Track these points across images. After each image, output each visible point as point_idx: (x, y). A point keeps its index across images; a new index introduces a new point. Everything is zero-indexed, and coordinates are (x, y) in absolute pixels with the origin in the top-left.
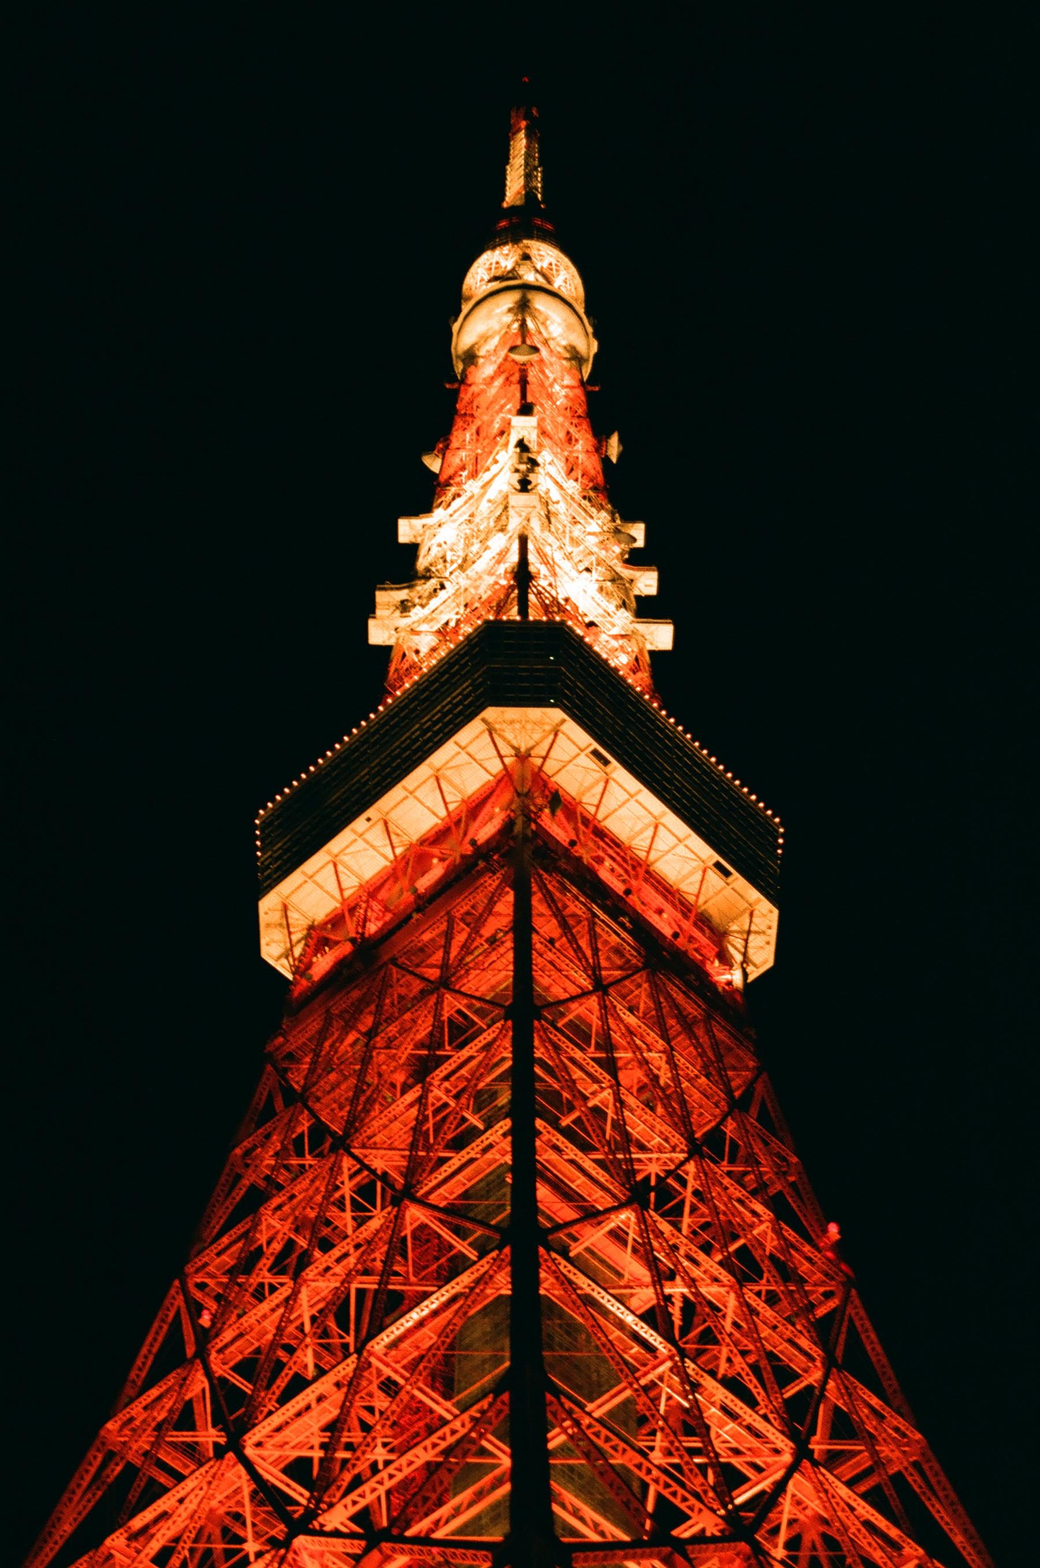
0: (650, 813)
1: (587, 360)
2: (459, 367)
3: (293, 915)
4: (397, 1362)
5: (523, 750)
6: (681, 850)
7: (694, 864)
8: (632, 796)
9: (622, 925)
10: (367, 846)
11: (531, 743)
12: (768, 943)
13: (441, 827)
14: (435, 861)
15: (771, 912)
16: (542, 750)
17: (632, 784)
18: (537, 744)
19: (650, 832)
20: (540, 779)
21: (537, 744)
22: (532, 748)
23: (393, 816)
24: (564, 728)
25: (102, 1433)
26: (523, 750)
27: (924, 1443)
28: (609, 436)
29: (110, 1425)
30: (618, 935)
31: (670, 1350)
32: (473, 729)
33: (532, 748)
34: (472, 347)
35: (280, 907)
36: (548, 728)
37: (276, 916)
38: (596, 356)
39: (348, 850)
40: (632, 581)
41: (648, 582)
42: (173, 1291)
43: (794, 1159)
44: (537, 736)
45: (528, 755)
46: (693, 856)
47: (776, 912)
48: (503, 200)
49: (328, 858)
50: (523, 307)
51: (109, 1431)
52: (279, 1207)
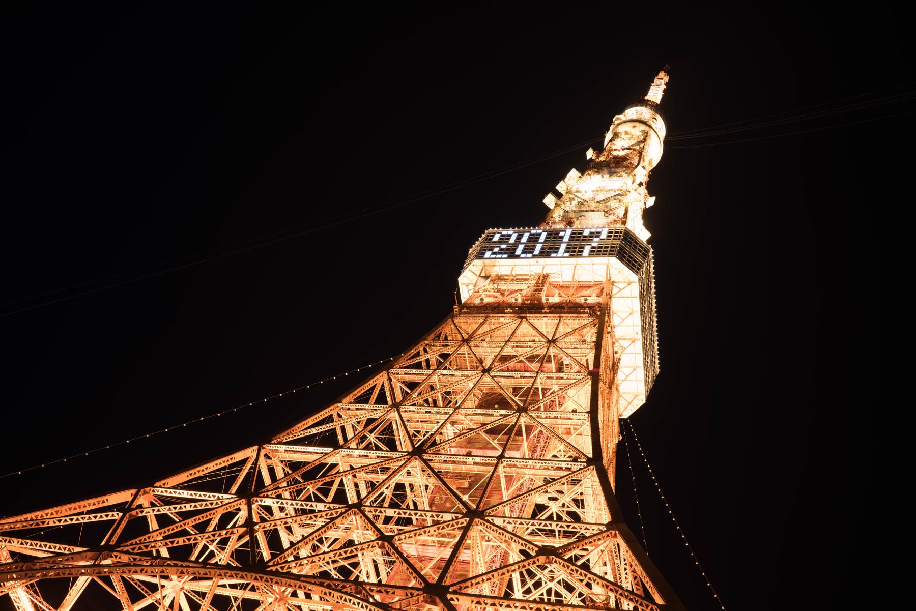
4: (504, 472)
5: (612, 280)
11: (617, 281)
12: (632, 410)
13: (561, 284)
14: (557, 295)
15: (642, 401)
16: (621, 286)
18: (619, 282)
20: (610, 296)
21: (619, 282)
22: (616, 282)
24: (633, 284)
25: (336, 405)
26: (612, 280)
29: (340, 405)
33: (616, 282)
34: (619, 133)
36: (627, 281)
39: (520, 267)
42: (381, 374)
44: (620, 280)
45: (613, 283)
46: (634, 363)
47: (644, 402)
48: (646, 95)
49: (513, 264)
51: (338, 407)
52: (443, 375)
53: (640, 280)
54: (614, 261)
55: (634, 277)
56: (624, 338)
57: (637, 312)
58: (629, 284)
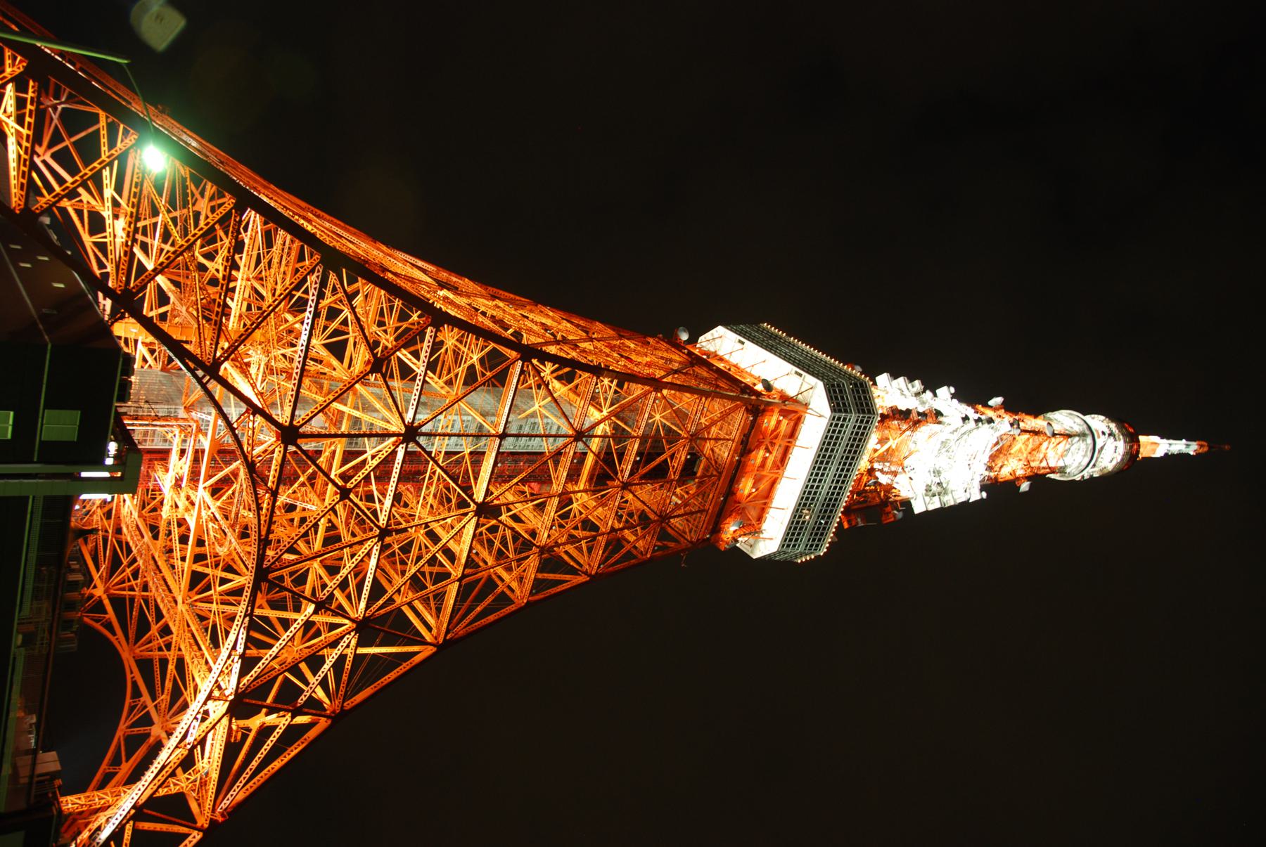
9: (733, 457)
27: (523, 604)
32: (810, 380)
38: (1074, 481)
43: (648, 556)
50: (1082, 435)
54: (820, 386)
55: (827, 412)
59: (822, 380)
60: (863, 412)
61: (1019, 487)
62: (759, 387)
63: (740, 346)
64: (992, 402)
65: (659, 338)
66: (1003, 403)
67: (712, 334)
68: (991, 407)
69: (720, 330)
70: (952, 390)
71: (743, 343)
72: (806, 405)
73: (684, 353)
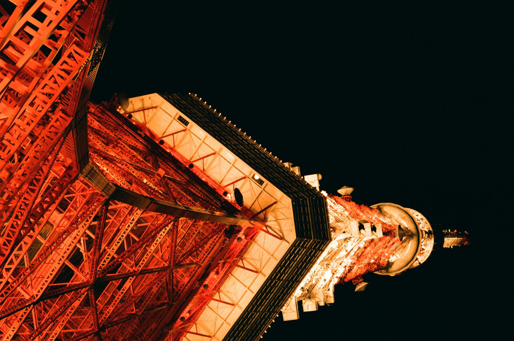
0: (239, 301)
1: (387, 271)
2: (374, 206)
3: (149, 113)
6: (220, 322)
7: (212, 330)
8: (248, 288)
10: (197, 148)
17: (256, 287)
19: (231, 302)
23: (218, 157)
24: (284, 243)
28: (364, 281)
30: (188, 282)
31: (37, 295)
35: (154, 105)
37: (147, 104)
40: (310, 298)
41: (309, 306)
53: (295, 242)
55: (291, 236)
56: (228, 294)
57: (264, 275)
58: (282, 238)
59: (288, 194)
60: (320, 239)
61: (355, 287)
62: (231, 197)
63: (179, 126)
64: (342, 191)
65: (103, 105)
66: (352, 194)
67: (143, 100)
68: (340, 195)
69: (155, 98)
70: (320, 177)
71: (186, 123)
72: (264, 220)
73: (140, 135)
